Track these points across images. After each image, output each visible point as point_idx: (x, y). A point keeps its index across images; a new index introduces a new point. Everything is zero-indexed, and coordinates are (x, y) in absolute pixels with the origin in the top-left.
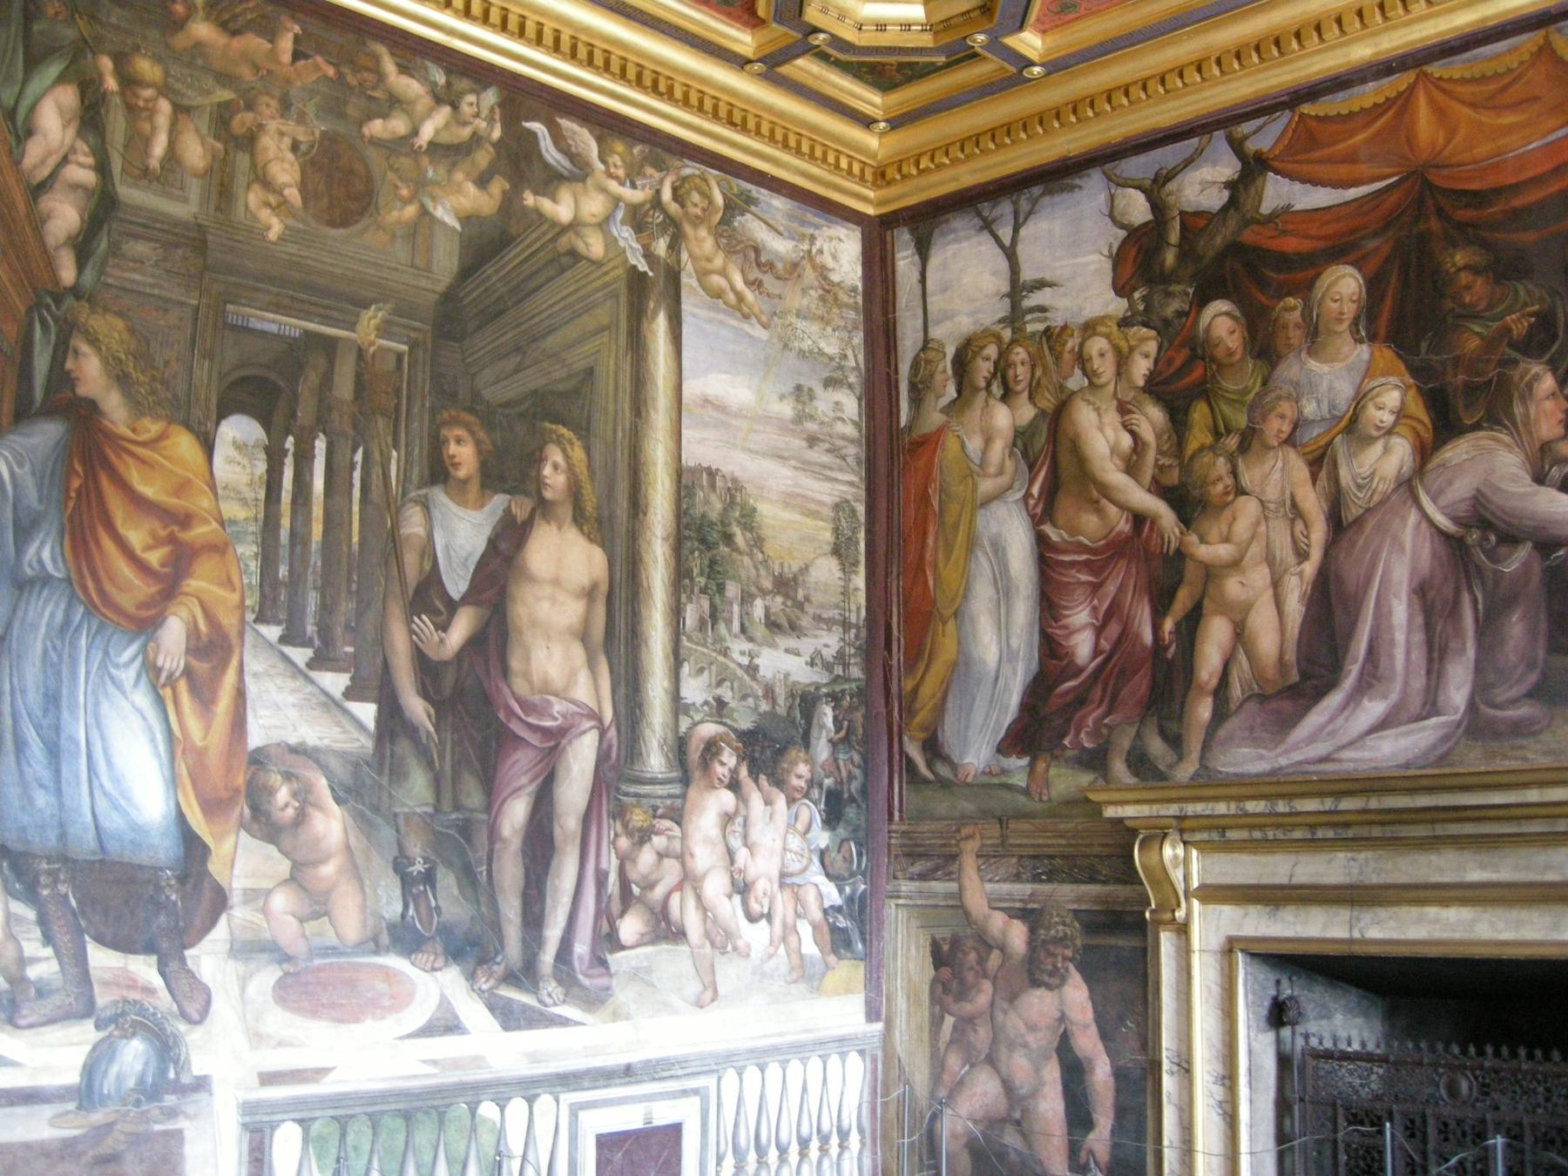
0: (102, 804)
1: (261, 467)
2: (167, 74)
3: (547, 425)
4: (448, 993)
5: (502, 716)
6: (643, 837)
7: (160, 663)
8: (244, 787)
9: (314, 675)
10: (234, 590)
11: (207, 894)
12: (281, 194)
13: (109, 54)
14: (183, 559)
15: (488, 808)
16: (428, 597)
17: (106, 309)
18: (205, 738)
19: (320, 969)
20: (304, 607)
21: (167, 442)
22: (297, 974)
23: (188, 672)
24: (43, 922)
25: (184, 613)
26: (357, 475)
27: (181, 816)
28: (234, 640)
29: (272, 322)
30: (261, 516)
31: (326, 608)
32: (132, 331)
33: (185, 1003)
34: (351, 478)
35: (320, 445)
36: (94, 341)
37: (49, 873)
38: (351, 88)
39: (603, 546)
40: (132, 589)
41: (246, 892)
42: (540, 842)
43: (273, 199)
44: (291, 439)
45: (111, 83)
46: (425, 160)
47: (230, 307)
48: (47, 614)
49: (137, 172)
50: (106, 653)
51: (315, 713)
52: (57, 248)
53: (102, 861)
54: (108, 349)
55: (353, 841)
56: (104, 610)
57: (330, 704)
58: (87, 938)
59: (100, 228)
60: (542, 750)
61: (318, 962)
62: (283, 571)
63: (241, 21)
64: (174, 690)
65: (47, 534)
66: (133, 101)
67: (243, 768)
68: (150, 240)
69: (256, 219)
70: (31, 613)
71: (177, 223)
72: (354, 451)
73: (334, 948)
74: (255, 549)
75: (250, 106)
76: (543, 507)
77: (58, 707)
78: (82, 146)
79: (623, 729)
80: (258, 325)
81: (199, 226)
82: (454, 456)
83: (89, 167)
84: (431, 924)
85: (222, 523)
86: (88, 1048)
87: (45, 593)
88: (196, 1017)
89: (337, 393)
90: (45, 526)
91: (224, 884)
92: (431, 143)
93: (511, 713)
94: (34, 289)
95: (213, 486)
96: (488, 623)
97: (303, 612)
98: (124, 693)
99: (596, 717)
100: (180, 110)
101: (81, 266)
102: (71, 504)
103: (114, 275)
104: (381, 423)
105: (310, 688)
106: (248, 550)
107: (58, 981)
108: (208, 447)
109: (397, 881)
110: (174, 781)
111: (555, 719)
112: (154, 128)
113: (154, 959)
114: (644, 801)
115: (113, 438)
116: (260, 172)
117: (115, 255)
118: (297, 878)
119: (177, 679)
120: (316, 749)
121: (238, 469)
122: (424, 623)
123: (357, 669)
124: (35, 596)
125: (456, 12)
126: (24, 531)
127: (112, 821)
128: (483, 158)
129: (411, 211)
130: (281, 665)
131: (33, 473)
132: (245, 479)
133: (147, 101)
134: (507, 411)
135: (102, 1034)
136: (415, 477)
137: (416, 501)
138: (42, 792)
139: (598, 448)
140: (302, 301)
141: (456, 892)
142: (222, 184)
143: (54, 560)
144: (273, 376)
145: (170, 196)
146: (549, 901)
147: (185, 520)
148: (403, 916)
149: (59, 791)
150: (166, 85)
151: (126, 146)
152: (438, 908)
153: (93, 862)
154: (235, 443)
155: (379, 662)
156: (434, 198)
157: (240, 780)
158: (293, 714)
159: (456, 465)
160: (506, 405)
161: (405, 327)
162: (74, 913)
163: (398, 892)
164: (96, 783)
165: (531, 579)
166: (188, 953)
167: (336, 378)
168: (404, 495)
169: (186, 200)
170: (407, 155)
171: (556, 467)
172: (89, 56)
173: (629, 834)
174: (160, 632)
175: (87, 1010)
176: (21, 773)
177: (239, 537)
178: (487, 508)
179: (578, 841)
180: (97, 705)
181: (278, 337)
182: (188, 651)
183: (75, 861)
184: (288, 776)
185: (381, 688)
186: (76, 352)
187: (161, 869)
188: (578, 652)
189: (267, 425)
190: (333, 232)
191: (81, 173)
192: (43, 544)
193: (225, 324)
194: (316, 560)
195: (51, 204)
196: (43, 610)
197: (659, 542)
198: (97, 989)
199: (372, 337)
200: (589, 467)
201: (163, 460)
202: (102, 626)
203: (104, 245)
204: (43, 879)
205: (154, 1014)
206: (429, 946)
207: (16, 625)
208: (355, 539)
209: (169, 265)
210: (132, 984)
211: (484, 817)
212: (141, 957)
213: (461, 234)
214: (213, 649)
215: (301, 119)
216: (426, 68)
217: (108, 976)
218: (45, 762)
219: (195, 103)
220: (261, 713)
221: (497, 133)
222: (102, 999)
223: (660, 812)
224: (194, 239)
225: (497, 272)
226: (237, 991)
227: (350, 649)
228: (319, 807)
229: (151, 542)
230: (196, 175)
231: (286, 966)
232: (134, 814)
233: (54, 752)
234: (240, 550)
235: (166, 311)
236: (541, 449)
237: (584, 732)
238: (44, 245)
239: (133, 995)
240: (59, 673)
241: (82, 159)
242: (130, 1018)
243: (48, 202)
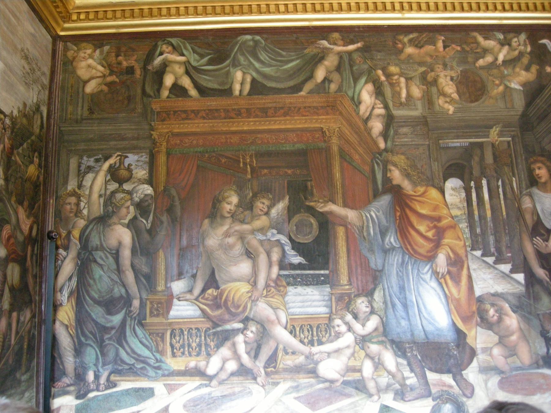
0: (425, 322)
1: (463, 195)
2: (401, 69)
7: (438, 271)
8: (477, 311)
9: (497, 266)
10: (461, 241)
11: (468, 350)
12: (451, 97)
13: (380, 69)
14: (440, 233)
17: (397, 153)
18: (459, 295)
20: (489, 242)
21: (427, 194)
22: (507, 378)
23: (449, 272)
24: (409, 364)
25: (444, 252)
26: (501, 190)
27: (454, 324)
28: (464, 258)
29: (457, 143)
30: (467, 212)
31: (497, 241)
32: (408, 158)
33: (464, 391)
35: (484, 182)
36: (395, 165)
37: (409, 348)
38: (468, 52)
40: (424, 246)
41: (482, 348)
43: (448, 100)
44: (472, 182)
45: (383, 78)
46: (502, 68)
47: (441, 141)
48: (396, 260)
49: (398, 105)
50: (418, 270)
51: (500, 280)
52: (377, 138)
53: (427, 342)
54: (401, 166)
55: (522, 326)
56: (415, 255)
57: (505, 276)
58: (426, 369)
59: (390, 126)
62: (478, 230)
63: (422, 43)
64: (445, 279)
65: (391, 233)
66: (391, 81)
67: (475, 304)
68: (407, 126)
69: (443, 108)
70: (390, 260)
71: (418, 117)
72: (498, 181)
74: (466, 224)
75: (432, 70)
77: (404, 291)
78: (378, 102)
80: (453, 145)
81: (424, 116)
82: (538, 175)
83: (382, 108)
85: (452, 217)
86: (431, 408)
87: (394, 253)
88: (469, 395)
90: (390, 231)
91: (474, 346)
92: (503, 61)
94: (372, 153)
95: (446, 205)
97: (489, 244)
98: (427, 283)
100: (408, 79)
101: (386, 141)
102: (398, 221)
103: (398, 141)
104: (506, 168)
105: (496, 271)
106: (464, 225)
107: (417, 385)
108: (443, 192)
110: (450, 312)
112: (401, 88)
113: (451, 375)
115: (409, 196)
116: (441, 92)
117: (396, 134)
118: (502, 341)
119: (445, 275)
120: (502, 294)
121: (455, 197)
122: (538, 240)
123: (513, 261)
124: (391, 255)
125: (500, 11)
126: (383, 233)
127: (429, 328)
128: (525, 60)
129: (501, 88)
130: (484, 265)
131: (383, 214)
132: (458, 200)
133: (396, 80)
135: (435, 403)
136: (524, 186)
137: (526, 195)
138: (403, 320)
140: (467, 132)
142: (428, 100)
143: (395, 241)
144: (461, 162)
145: (411, 109)
147: (439, 219)
149: (409, 320)
150: (402, 73)
151: (392, 97)
153: (424, 343)
154: (453, 189)
155: (522, 257)
156: (509, 81)
157: (474, 308)
158: (491, 282)
159: (540, 178)
161: (508, 131)
162: (420, 361)
164: (421, 315)
166: (463, 372)
167: (485, 157)
168: (521, 193)
169: (417, 109)
170: (495, 68)
172: (374, 71)
174: (436, 260)
175: (429, 394)
176: (395, 315)
177: (459, 221)
180: (418, 288)
181: (461, 147)
182: (448, 265)
183: (418, 343)
184: (493, 305)
186: (390, 170)
187: (449, 343)
189: (462, 179)
190: (473, 105)
191: (380, 111)
192: (390, 236)
193: (440, 148)
194: (490, 224)
195: (372, 124)
196: (394, 258)
198: (431, 387)
199: (496, 138)
201: (427, 199)
202: (415, 261)
203: (392, 132)
204: (407, 350)
205: (454, 395)
207: (386, 265)
208: (504, 213)
209: (416, 133)
210: (444, 385)
212: (446, 375)
213: (523, 91)
214: (457, 263)
215: (452, 69)
216: (495, 35)
217: (434, 382)
218: (403, 310)
219: (413, 75)
220: (479, 283)
221: (529, 49)
222: (434, 390)
224: (423, 121)
225: (541, 101)
226: (483, 385)
227: (509, 255)
228: (506, 315)
229: (428, 229)
230: (419, 100)
231: (502, 375)
232: (437, 325)
233: (405, 306)
234: (461, 226)
235: (418, 148)
238: (372, 138)
239: (445, 388)
240: (403, 280)
241: (379, 106)
242: (444, 397)
243: (370, 124)
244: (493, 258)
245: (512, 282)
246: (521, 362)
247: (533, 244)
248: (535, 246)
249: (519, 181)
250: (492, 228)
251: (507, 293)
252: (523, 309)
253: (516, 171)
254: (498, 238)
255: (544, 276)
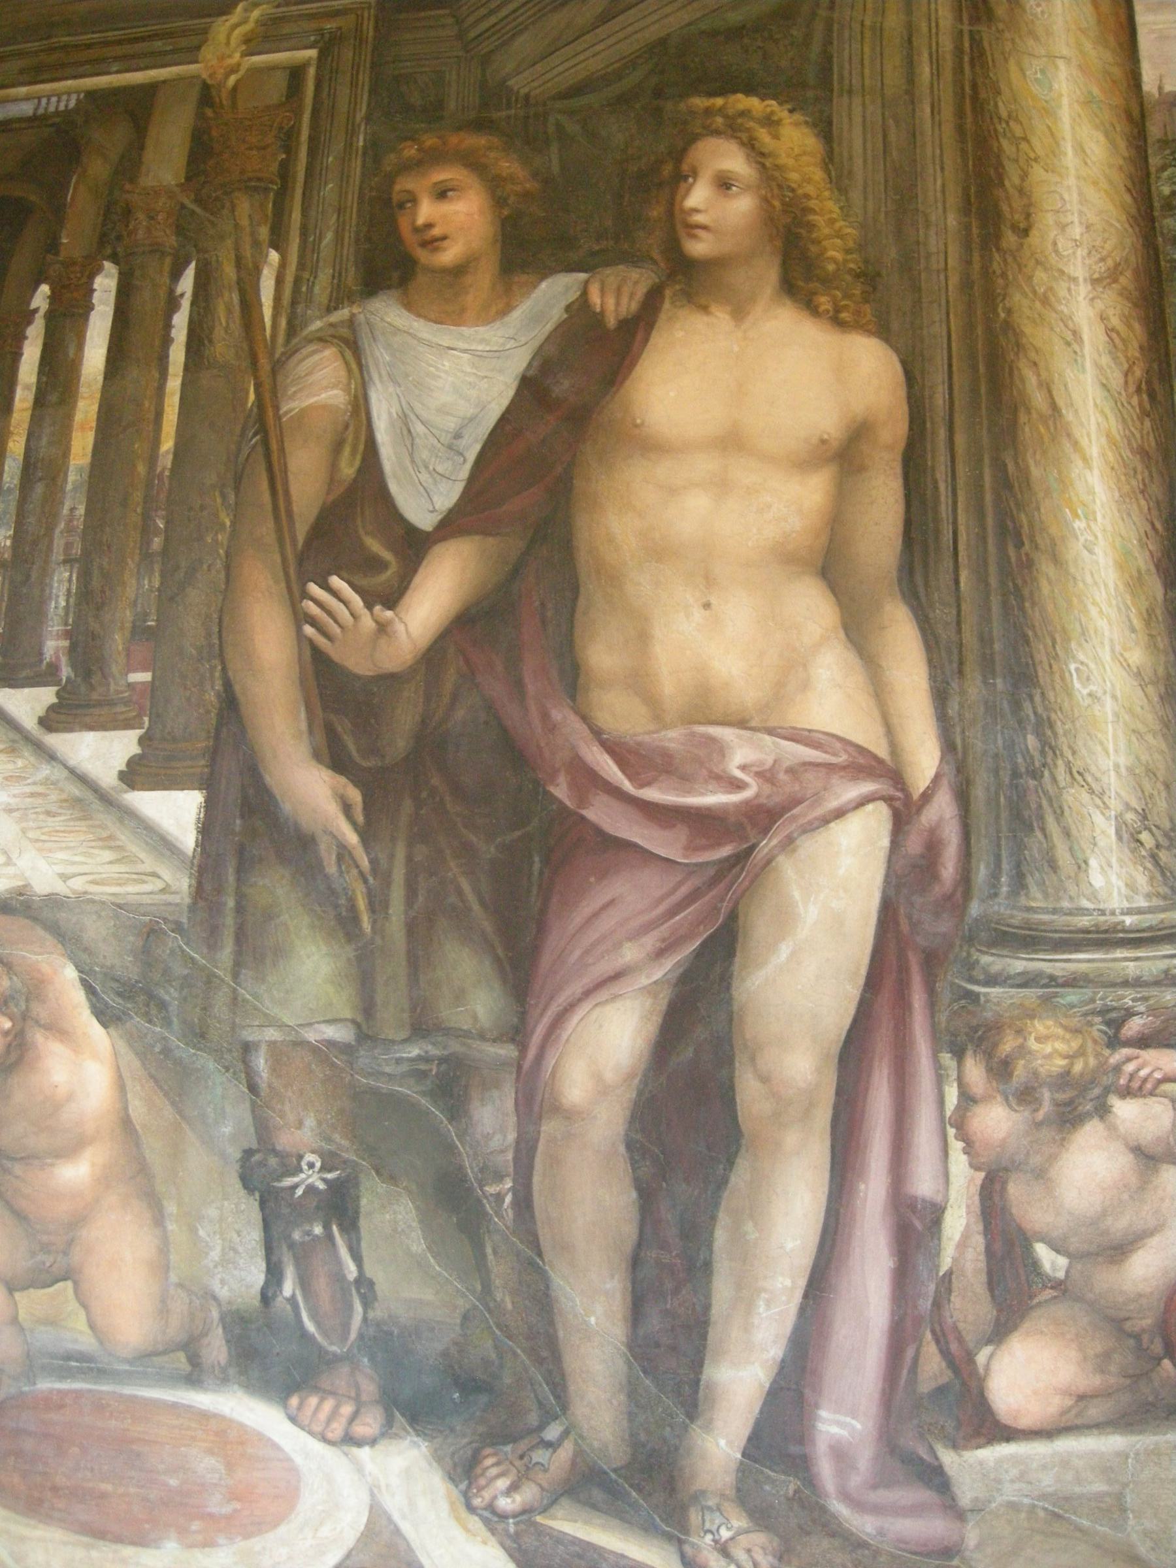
3: (699, 102)
4: (394, 1504)
5: (561, 790)
6: (1075, 1104)
9: (54, 740)
15: (517, 1034)
16: (358, 534)
19: (52, 1403)
20: (43, 602)
26: (181, 320)
31: (91, 598)
34: (168, 326)
35: (105, 285)
39: (883, 331)
42: (690, 1115)
44: (45, 289)
55: (137, 1110)
57: (90, 799)
60: (692, 870)
61: (45, 1385)
72: (176, 275)
73: (82, 1357)
76: (687, 279)
79: (979, 793)
82: (429, 226)
84: (346, 1327)
89: (147, 181)
93: (588, 781)
96: (516, 572)
97: (40, 614)
99: (886, 772)
104: (244, 206)
105: (46, 770)
109: (251, 1208)
111: (738, 785)
114: (1071, 996)
120: (54, 901)
122: (339, 598)
123: (156, 718)
134: (575, 103)
137: (322, 339)
139: (856, 120)
141: (418, 1246)
146: (722, 1290)
148: (266, 1297)
152: (364, 1284)
159: (433, 244)
160: (578, 90)
163: (254, 1235)
165: (651, 447)
168: (292, 331)
171: (724, 184)
173: (1026, 1096)
178: (516, 314)
179: (823, 1116)
185: (214, 754)
188: (811, 608)
194: (74, 504)
197: (1083, 290)
200: (829, 159)
206: (340, 1378)
211: (507, 1051)
223: (1134, 1026)
227: (143, 677)
228: (59, 1030)
236: (679, 154)
237: (840, 814)
244: (47, 696)
245: (124, 838)
246: (92, 1326)
247: (301, 618)
248: (309, 630)
249: (301, 266)
250: (79, 523)
251: (83, 901)
252: (163, 1005)
253: (296, 216)
254: (96, 583)
255: (332, 809)
